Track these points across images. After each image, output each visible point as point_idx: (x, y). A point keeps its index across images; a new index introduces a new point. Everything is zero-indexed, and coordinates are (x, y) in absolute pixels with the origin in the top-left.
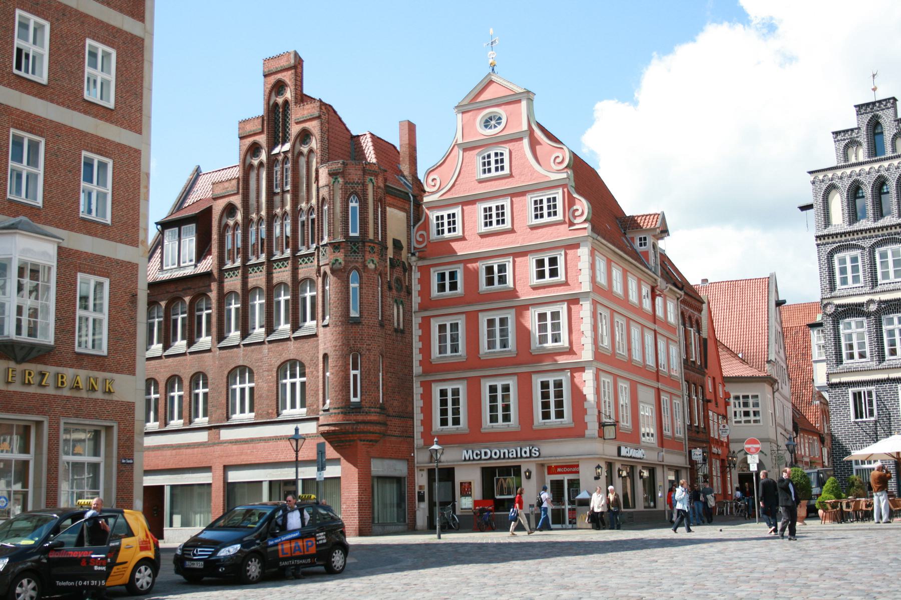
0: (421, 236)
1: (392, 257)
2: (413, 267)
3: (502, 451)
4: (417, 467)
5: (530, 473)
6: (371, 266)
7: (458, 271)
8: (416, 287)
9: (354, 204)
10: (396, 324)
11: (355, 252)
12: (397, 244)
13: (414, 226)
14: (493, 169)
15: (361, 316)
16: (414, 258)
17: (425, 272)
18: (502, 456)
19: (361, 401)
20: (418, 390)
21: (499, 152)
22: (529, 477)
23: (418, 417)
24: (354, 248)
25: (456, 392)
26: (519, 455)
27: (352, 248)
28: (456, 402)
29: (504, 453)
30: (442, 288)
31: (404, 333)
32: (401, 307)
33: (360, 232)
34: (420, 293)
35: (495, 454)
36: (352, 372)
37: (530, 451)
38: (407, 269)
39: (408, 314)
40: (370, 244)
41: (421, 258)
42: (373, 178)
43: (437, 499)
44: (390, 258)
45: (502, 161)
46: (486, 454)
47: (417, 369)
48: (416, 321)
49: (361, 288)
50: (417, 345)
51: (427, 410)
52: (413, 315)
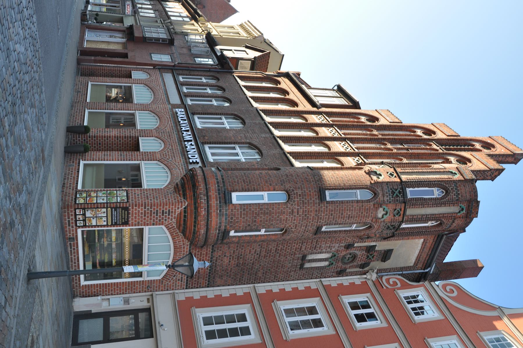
0: (395, 284)
1: (377, 248)
2: (365, 276)
4: (152, 295)
6: (380, 213)
7: (379, 322)
8: (345, 280)
9: (437, 193)
10: (310, 257)
11: (393, 193)
12: (386, 255)
13: (401, 275)
15: (328, 202)
17: (363, 288)
20: (240, 290)
23: (211, 292)
24: (397, 192)
27: (396, 190)
32: (327, 263)
34: (341, 285)
39: (321, 273)
40: (403, 209)
42: (464, 211)
44: (375, 246)
47: (262, 288)
48: (313, 283)
49: (358, 201)
50: (288, 286)
51: (219, 301)
52: (318, 280)
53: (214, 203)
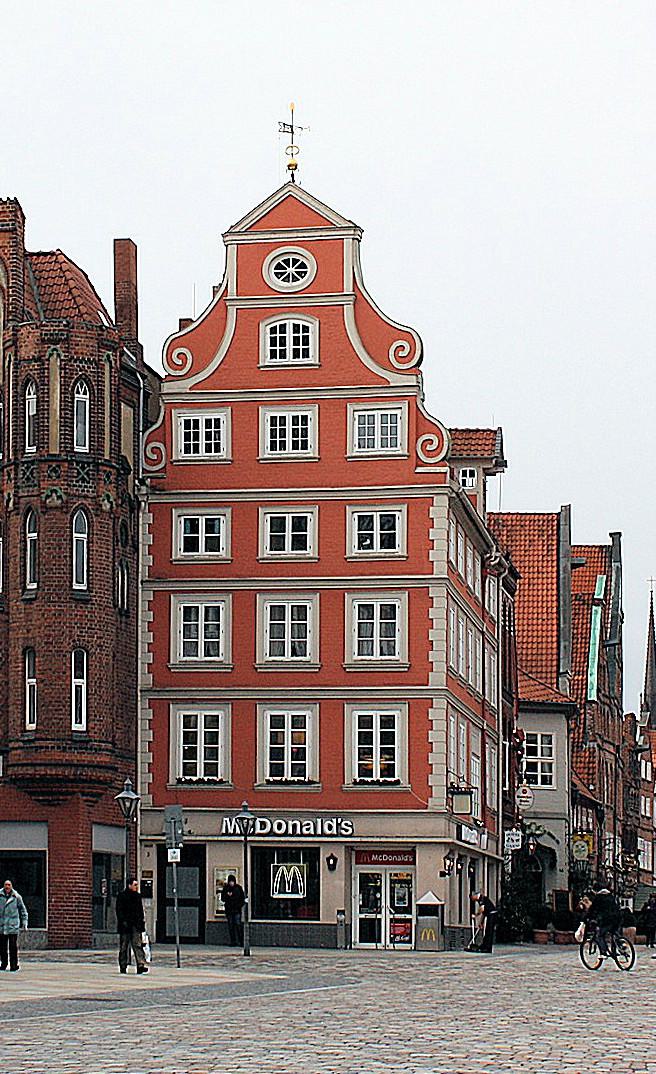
3: (290, 823)
4: (141, 841)
5: (335, 860)
6: (106, 506)
8: (145, 539)
9: (82, 396)
11: (83, 480)
13: (143, 432)
14: (290, 353)
16: (144, 490)
17: (162, 515)
18: (290, 831)
19: (87, 731)
20: (144, 713)
21: (301, 323)
22: (332, 868)
23: (144, 758)
25: (212, 721)
26: (319, 832)
27: (79, 473)
28: (212, 738)
29: (294, 826)
30: (191, 544)
31: (127, 614)
33: (90, 446)
35: (280, 826)
36: (75, 682)
37: (338, 825)
38: (134, 507)
39: (133, 579)
40: (105, 468)
41: (153, 488)
43: (173, 892)
45: (306, 341)
46: (263, 825)
47: (144, 679)
48: (144, 597)
50: (145, 637)
53: (86, 758)
